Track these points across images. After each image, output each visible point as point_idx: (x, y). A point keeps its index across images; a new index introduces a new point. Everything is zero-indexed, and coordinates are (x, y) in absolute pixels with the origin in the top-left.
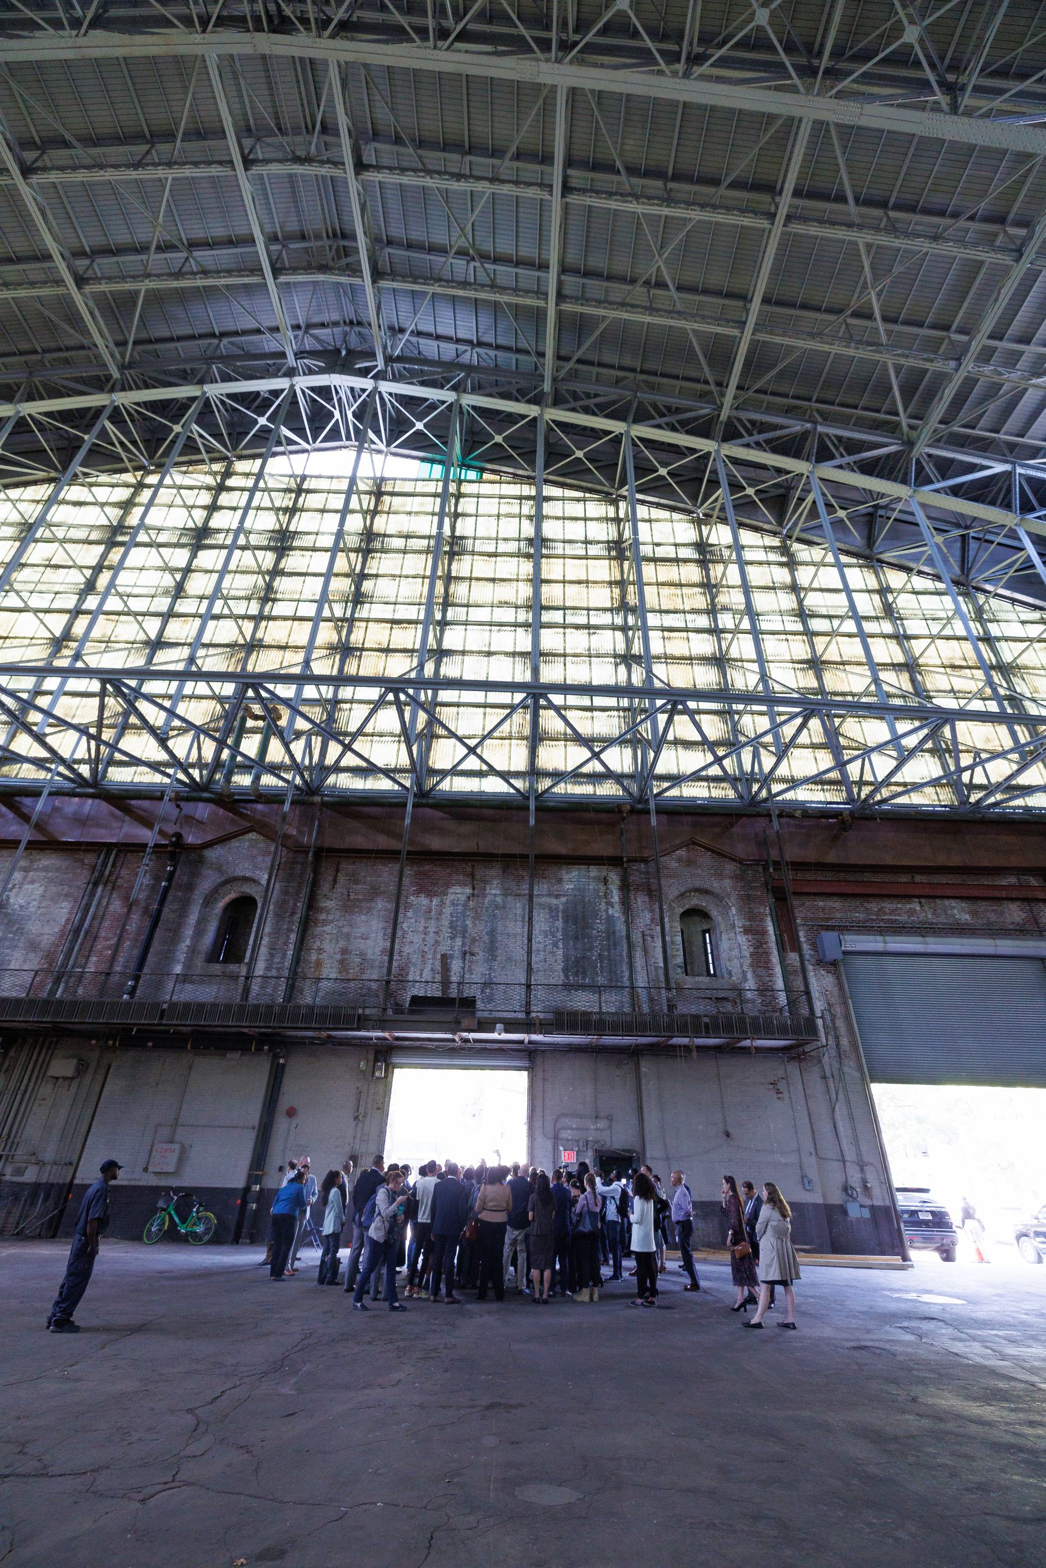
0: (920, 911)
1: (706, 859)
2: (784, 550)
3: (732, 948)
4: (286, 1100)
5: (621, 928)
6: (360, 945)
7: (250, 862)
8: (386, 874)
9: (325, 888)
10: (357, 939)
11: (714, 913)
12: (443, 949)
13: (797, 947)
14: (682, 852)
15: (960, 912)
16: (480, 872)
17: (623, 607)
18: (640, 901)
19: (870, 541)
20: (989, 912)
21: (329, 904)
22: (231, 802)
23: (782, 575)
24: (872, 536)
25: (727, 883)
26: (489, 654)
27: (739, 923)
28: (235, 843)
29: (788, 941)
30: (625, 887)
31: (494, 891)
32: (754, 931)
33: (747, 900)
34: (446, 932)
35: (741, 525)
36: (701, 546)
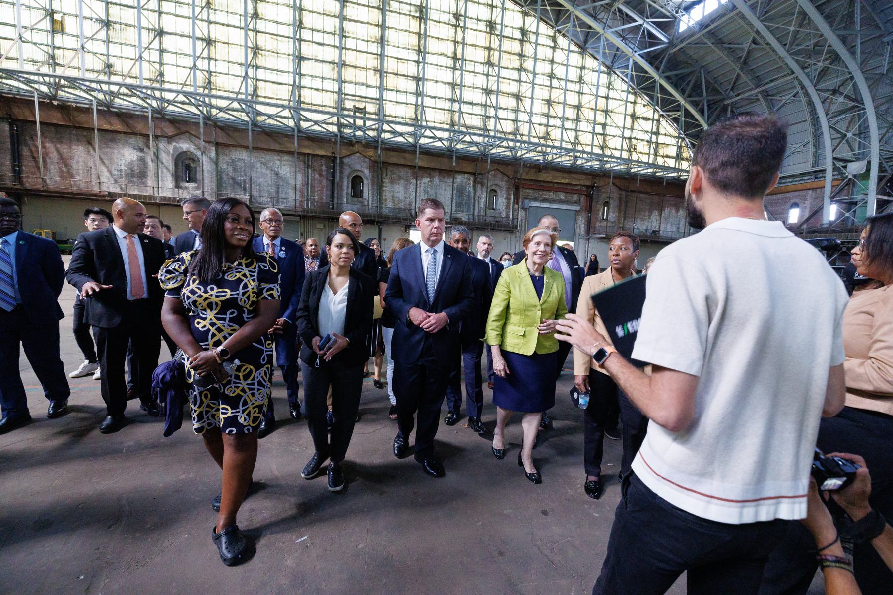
0: (552, 195)
1: (499, 175)
2: (554, 40)
3: (501, 202)
4: (383, 237)
5: (472, 195)
6: (397, 195)
7: (359, 165)
8: (403, 172)
9: (384, 175)
10: (399, 192)
11: (498, 192)
12: (422, 197)
13: (518, 203)
14: (493, 172)
15: (562, 196)
16: (432, 173)
17: (489, 63)
18: (479, 187)
19: (586, 42)
20: (569, 197)
21: (386, 181)
25: (504, 184)
26: (437, 82)
27: (505, 196)
28: (353, 157)
29: (516, 201)
30: (475, 182)
31: (436, 180)
32: (508, 199)
33: (508, 189)
34: (422, 192)
35: (541, 19)
36: (523, 31)
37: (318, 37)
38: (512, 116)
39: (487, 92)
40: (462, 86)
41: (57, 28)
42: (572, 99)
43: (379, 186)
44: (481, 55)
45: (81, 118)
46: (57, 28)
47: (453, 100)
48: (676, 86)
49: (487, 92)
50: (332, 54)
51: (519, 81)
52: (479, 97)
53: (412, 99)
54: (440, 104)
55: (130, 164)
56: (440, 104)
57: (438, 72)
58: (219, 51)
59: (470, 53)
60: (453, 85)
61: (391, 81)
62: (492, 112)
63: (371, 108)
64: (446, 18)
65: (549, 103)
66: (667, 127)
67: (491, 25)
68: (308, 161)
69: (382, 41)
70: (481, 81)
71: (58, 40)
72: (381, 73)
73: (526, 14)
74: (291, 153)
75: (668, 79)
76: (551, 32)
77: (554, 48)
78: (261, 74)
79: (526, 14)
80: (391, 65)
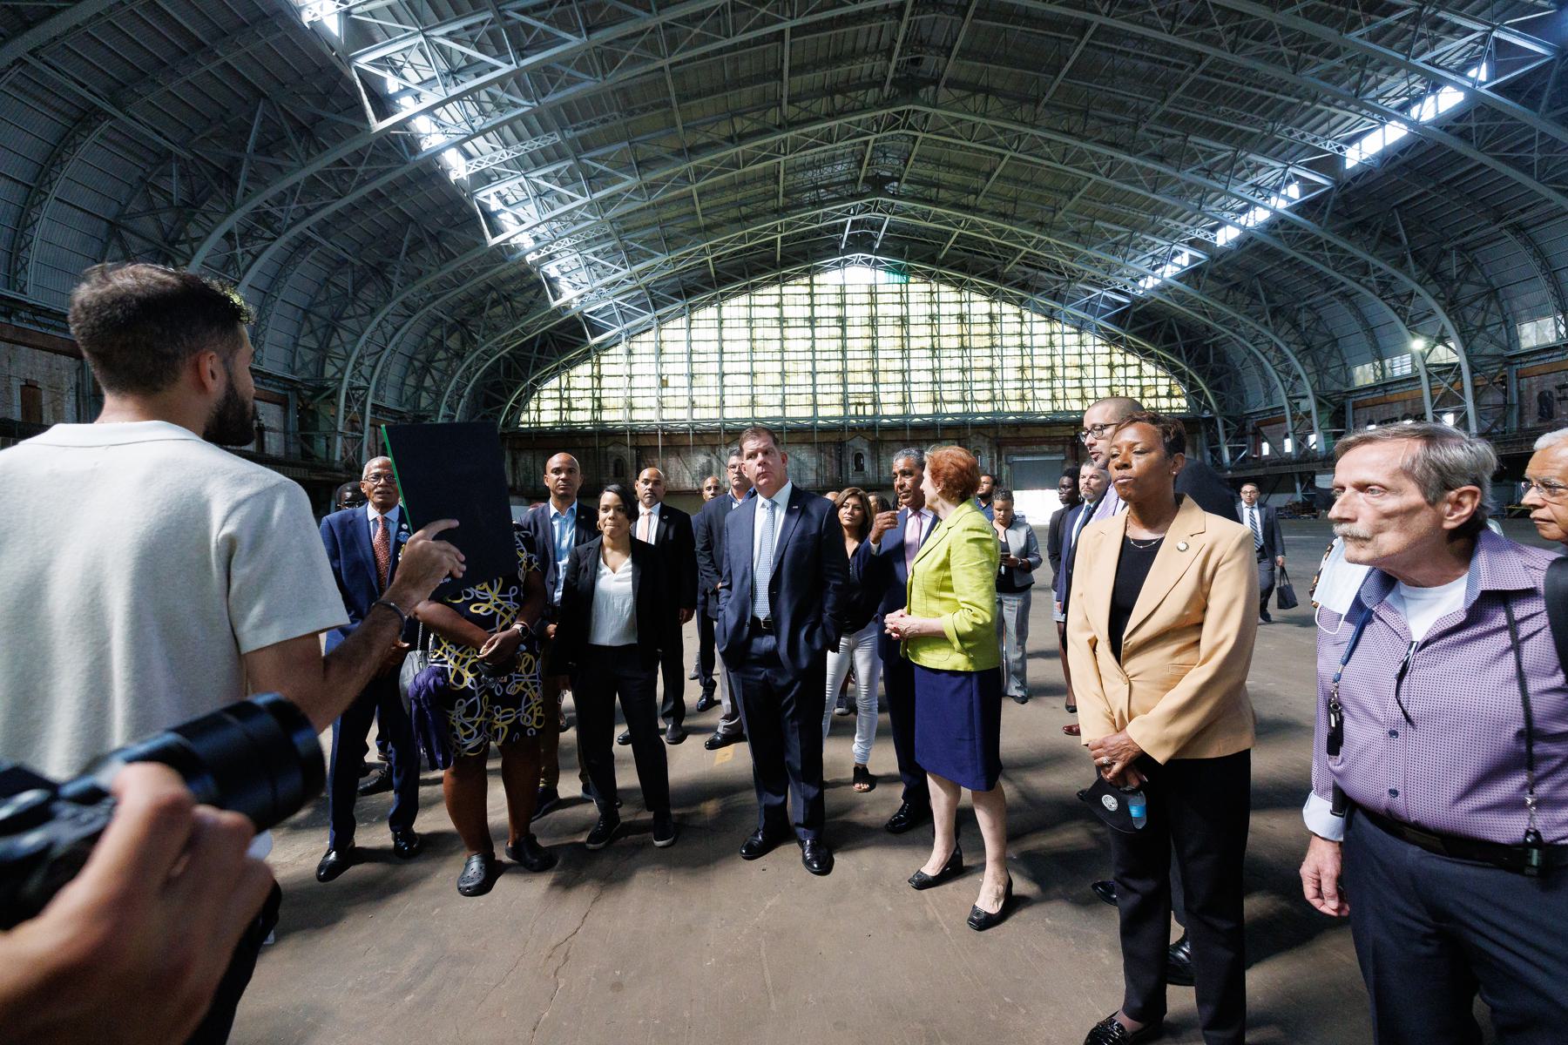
2: (1021, 316)
15: (1046, 448)
17: (963, 347)
22: (853, 429)
23: (1017, 328)
24: (1051, 316)
29: (999, 458)
36: (991, 315)
37: (825, 356)
38: (988, 386)
39: (963, 370)
40: (940, 370)
41: (664, 384)
42: (1047, 362)
43: (876, 458)
44: (955, 342)
45: (676, 440)
46: (664, 384)
47: (934, 382)
48: (1148, 340)
49: (963, 370)
50: (838, 366)
51: (992, 356)
52: (956, 376)
53: (900, 387)
54: (923, 387)
55: (702, 466)
56: (923, 387)
57: (920, 362)
58: (760, 379)
59: (945, 342)
60: (933, 371)
61: (882, 377)
62: (967, 386)
63: (868, 401)
64: (922, 320)
65: (1022, 369)
66: (1149, 369)
67: (961, 317)
68: (820, 447)
69: (874, 349)
70: (957, 363)
71: (665, 391)
72: (874, 372)
73: (991, 301)
74: (812, 444)
75: (1136, 334)
76: (1017, 310)
77: (1022, 323)
78: (787, 390)
79: (991, 301)
80: (882, 365)
